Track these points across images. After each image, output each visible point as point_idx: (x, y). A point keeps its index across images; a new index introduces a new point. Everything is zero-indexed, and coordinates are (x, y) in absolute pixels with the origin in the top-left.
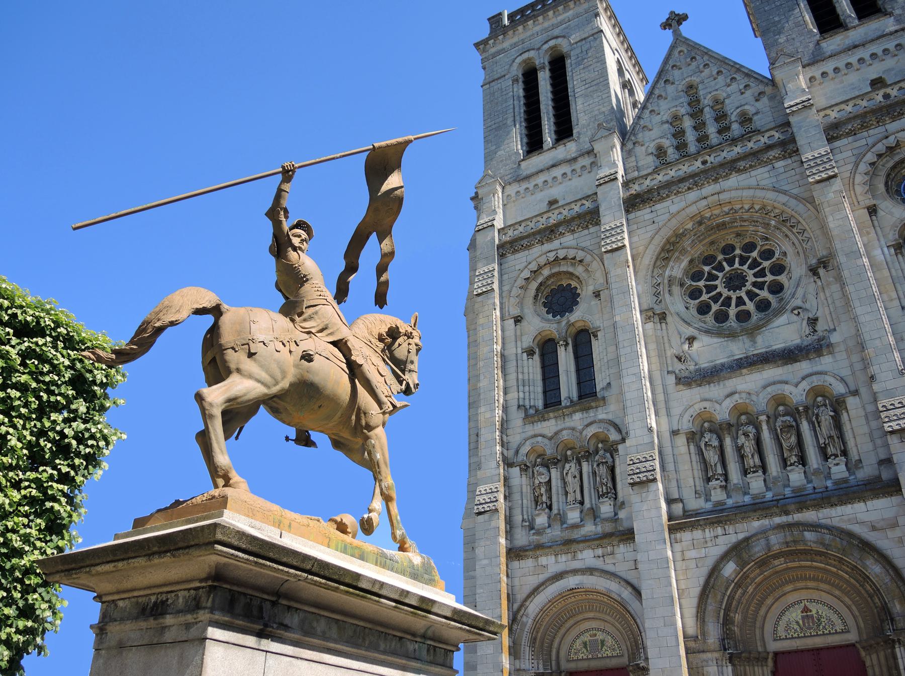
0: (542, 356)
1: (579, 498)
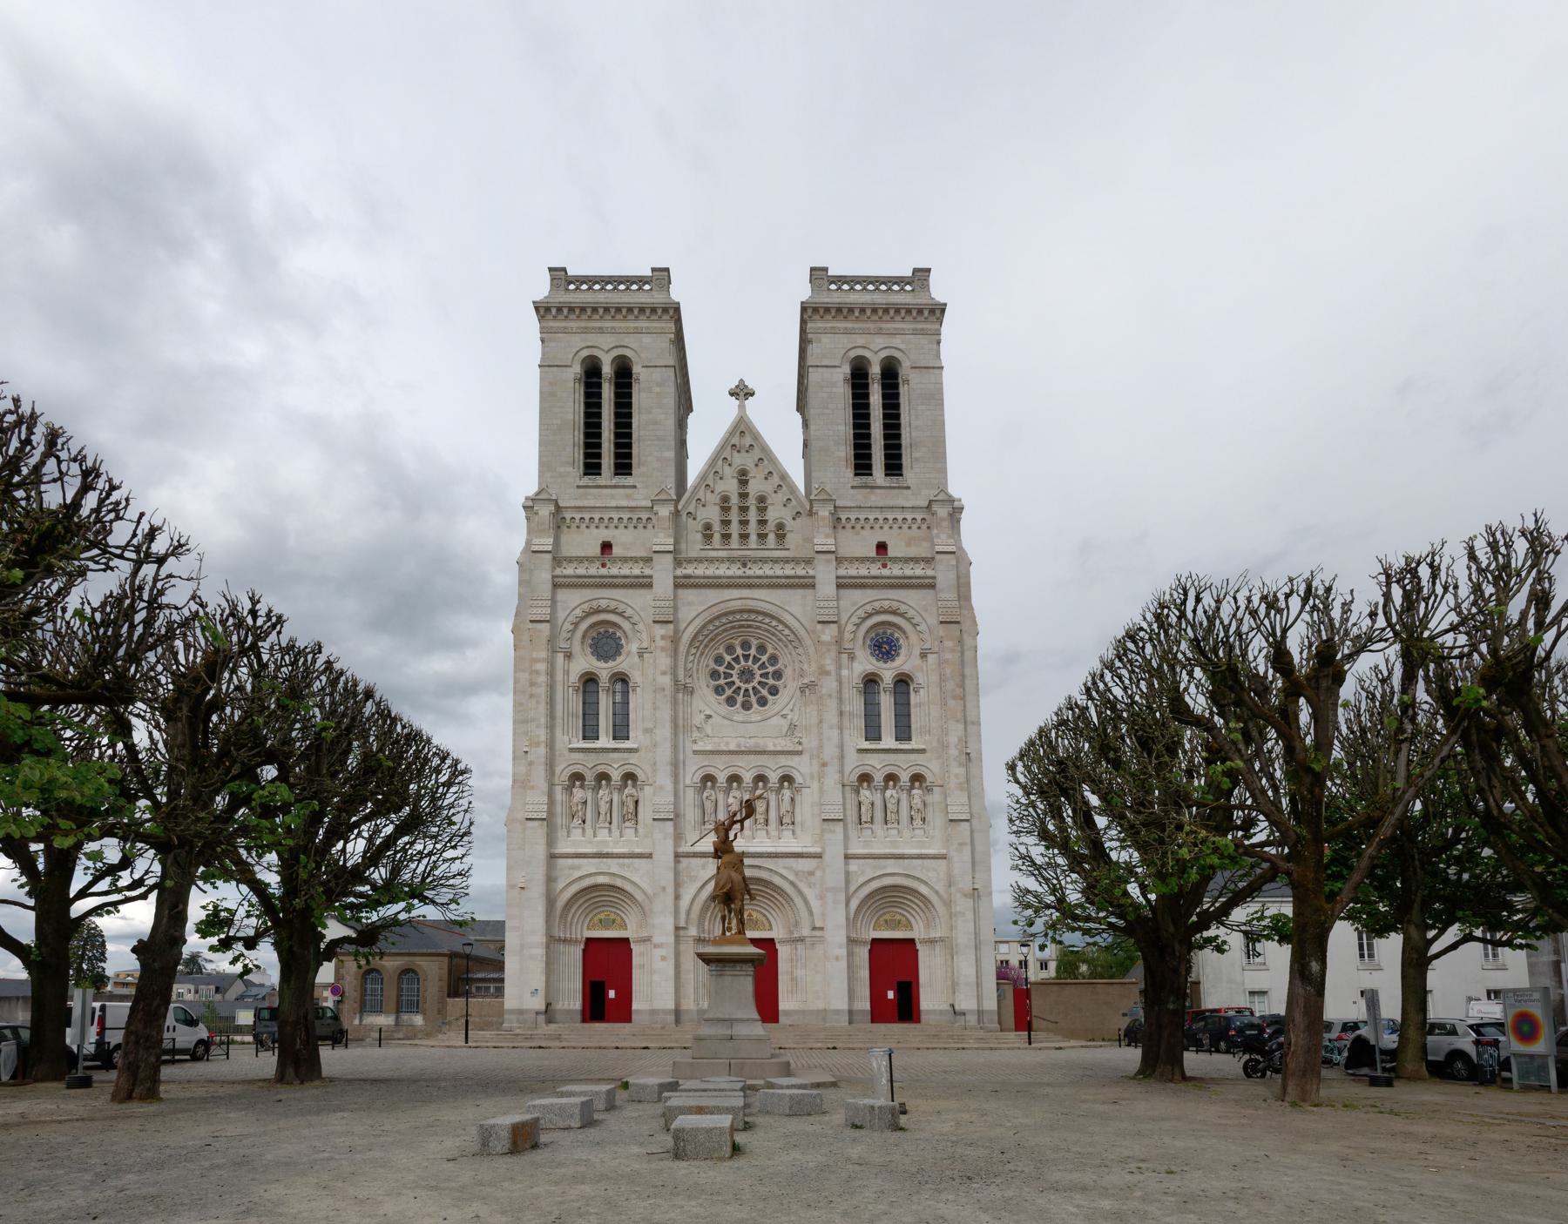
0: (584, 692)
1: (609, 819)
